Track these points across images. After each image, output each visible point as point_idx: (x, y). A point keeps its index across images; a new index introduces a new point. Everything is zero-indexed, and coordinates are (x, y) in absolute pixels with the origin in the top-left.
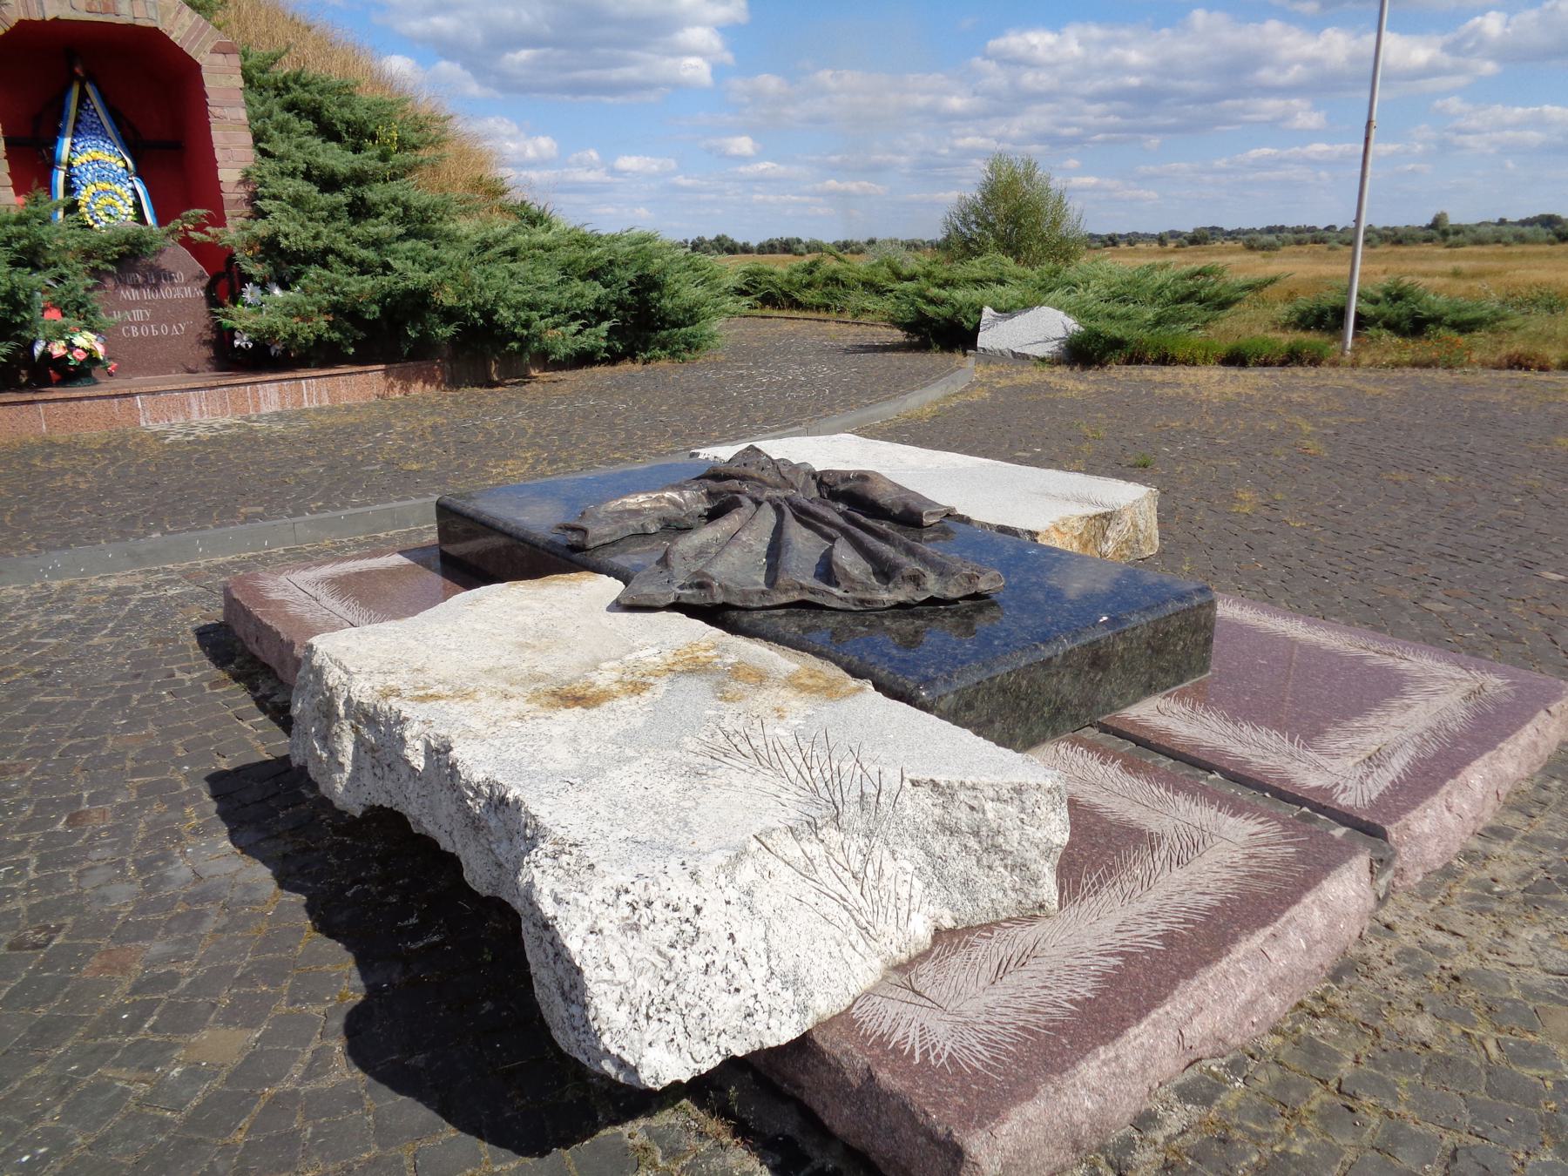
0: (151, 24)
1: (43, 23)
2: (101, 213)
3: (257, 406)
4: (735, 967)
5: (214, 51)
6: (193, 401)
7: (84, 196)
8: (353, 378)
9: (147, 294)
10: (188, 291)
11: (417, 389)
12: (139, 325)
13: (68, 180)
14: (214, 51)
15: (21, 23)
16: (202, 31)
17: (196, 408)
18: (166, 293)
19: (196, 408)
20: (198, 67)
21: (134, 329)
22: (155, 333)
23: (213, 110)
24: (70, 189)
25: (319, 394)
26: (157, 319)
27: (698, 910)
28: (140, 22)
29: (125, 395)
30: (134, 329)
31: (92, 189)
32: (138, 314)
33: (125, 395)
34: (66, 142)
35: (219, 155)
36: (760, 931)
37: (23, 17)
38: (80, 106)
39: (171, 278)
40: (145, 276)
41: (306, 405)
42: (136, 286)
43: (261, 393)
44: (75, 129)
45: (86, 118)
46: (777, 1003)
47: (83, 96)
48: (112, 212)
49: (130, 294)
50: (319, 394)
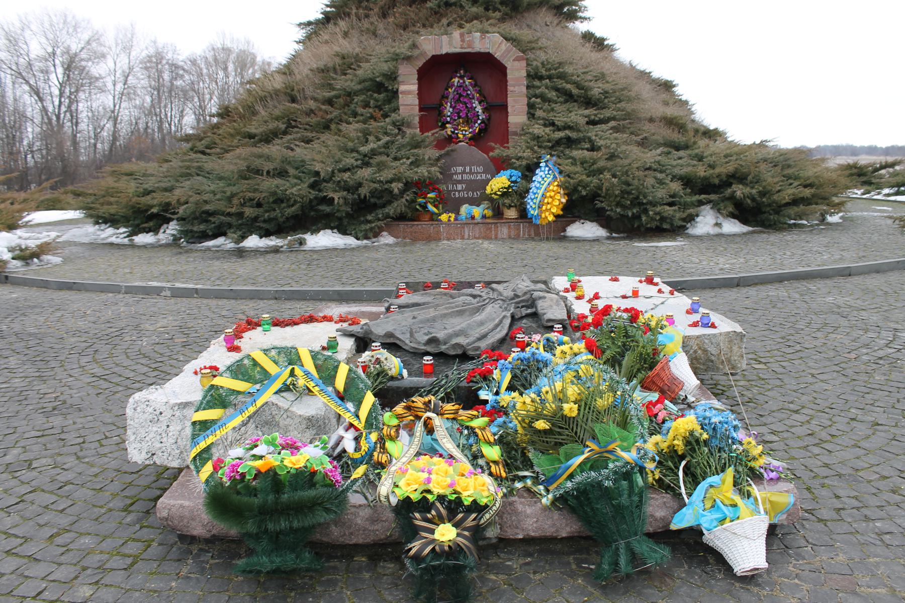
1: (442, 55)
4: (164, 435)
5: (514, 60)
12: (459, 191)
14: (514, 60)
15: (433, 56)
16: (509, 52)
20: (506, 68)
22: (466, 196)
23: (510, 88)
26: (467, 190)
27: (161, 413)
28: (482, 51)
32: (459, 187)
36: (179, 428)
46: (173, 453)
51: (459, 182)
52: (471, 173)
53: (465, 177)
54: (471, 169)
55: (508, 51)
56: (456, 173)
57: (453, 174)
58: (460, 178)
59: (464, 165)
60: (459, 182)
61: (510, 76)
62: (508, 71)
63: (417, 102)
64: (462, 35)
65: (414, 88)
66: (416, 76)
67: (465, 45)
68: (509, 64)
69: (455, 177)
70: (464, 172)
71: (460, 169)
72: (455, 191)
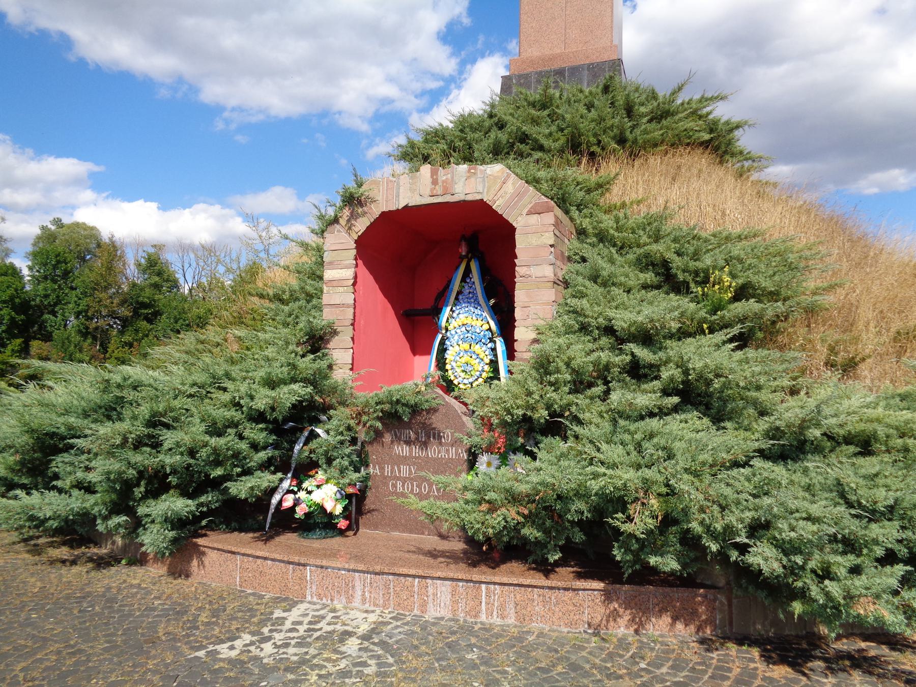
0: (478, 197)
2: (459, 370)
3: (424, 606)
6: (358, 584)
7: (450, 355)
8: (554, 595)
9: (416, 451)
10: (452, 451)
11: (659, 627)
12: (404, 480)
13: (442, 343)
14: (530, 213)
17: (359, 593)
18: (434, 451)
19: (359, 593)
20: (513, 229)
21: (399, 484)
24: (443, 350)
25: (502, 607)
28: (470, 198)
29: (299, 564)
30: (399, 484)
31: (457, 348)
32: (405, 471)
33: (299, 564)
34: (447, 311)
35: (518, 314)
37: (385, 209)
38: (463, 280)
39: (440, 438)
40: (417, 433)
41: (483, 617)
42: (408, 442)
43: (431, 590)
44: (457, 298)
45: (466, 290)
47: (467, 272)
48: (469, 368)
49: (402, 450)
50: (502, 607)
55: (519, 195)
61: (522, 243)
62: (517, 237)
64: (434, 173)
67: (439, 190)
68: (520, 221)
72: (398, 479)
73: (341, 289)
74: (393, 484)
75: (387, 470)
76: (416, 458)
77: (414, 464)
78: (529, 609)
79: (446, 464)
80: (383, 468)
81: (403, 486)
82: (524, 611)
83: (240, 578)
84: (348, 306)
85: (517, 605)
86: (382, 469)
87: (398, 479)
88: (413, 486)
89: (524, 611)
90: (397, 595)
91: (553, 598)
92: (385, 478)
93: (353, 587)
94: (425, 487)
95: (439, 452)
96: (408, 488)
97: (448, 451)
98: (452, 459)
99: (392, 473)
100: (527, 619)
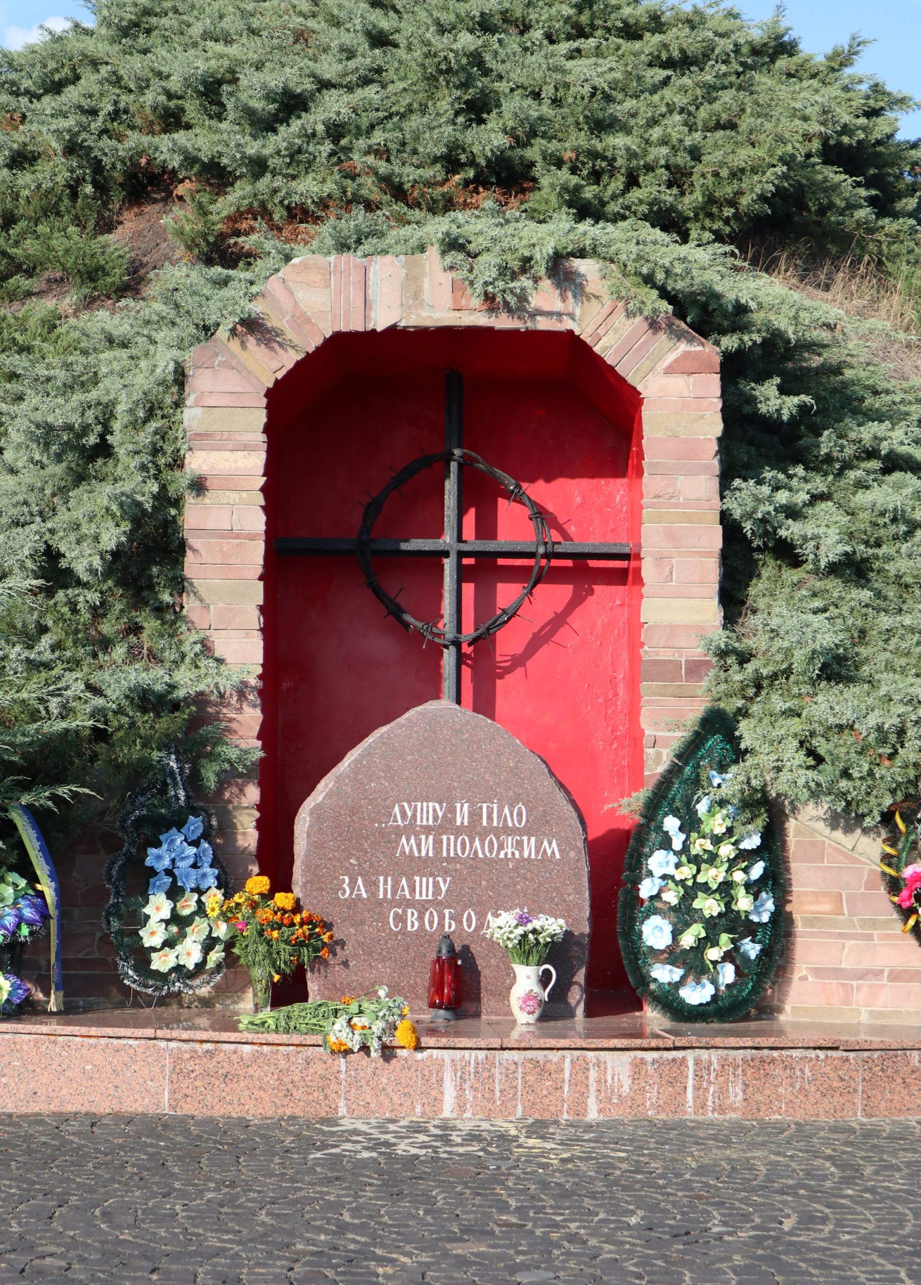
12: (422, 907)
21: (412, 916)
26: (457, 900)
30: (412, 916)
32: (424, 888)
51: (424, 866)
52: (474, 829)
53: (451, 845)
54: (475, 815)
56: (411, 829)
57: (399, 832)
58: (427, 846)
59: (448, 799)
60: (424, 866)
63: (258, 522)
65: (253, 463)
66: (262, 417)
69: (407, 845)
70: (445, 826)
71: (428, 812)
72: (410, 904)
73: (233, 496)
74: (396, 915)
75: (384, 887)
76: (448, 859)
77: (445, 873)
78: (767, 1092)
79: (516, 869)
80: (376, 884)
81: (421, 918)
82: (758, 1097)
83: (173, 1092)
84: (252, 537)
85: (747, 1086)
86: (372, 885)
87: (410, 904)
88: (442, 917)
89: (758, 1097)
90: (530, 1089)
91: (807, 1070)
92: (380, 903)
93: (440, 1081)
94: (469, 919)
95: (501, 847)
96: (431, 923)
97: (519, 845)
98: (529, 859)
99: (394, 892)
100: (763, 1108)
